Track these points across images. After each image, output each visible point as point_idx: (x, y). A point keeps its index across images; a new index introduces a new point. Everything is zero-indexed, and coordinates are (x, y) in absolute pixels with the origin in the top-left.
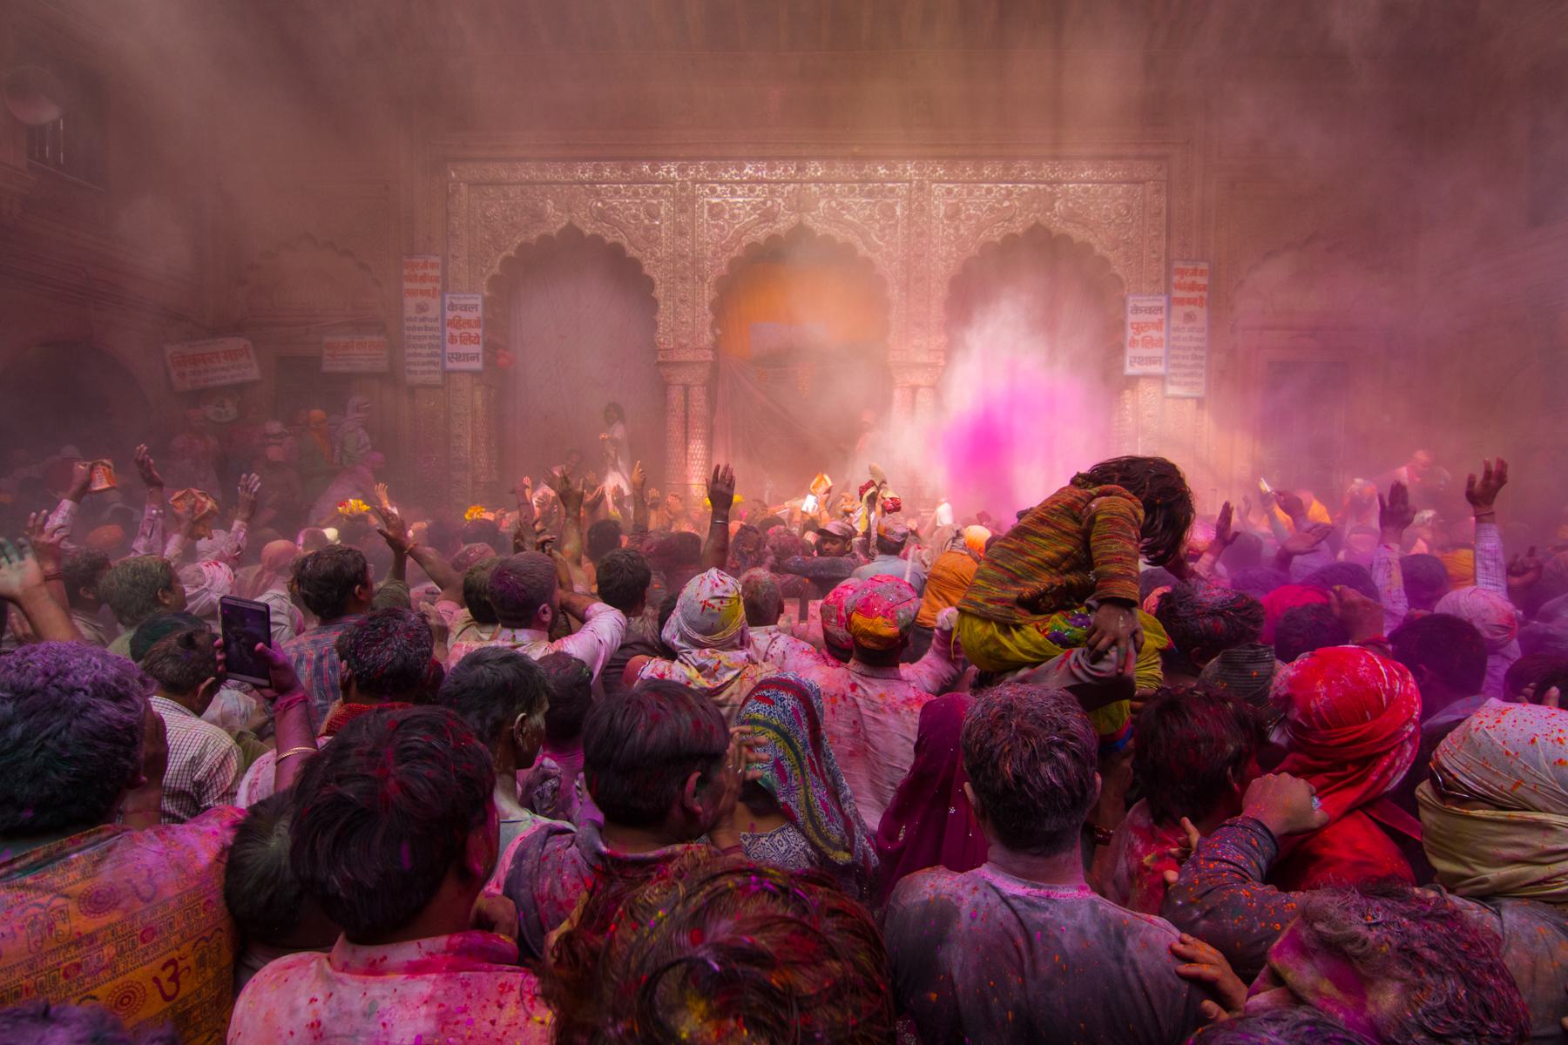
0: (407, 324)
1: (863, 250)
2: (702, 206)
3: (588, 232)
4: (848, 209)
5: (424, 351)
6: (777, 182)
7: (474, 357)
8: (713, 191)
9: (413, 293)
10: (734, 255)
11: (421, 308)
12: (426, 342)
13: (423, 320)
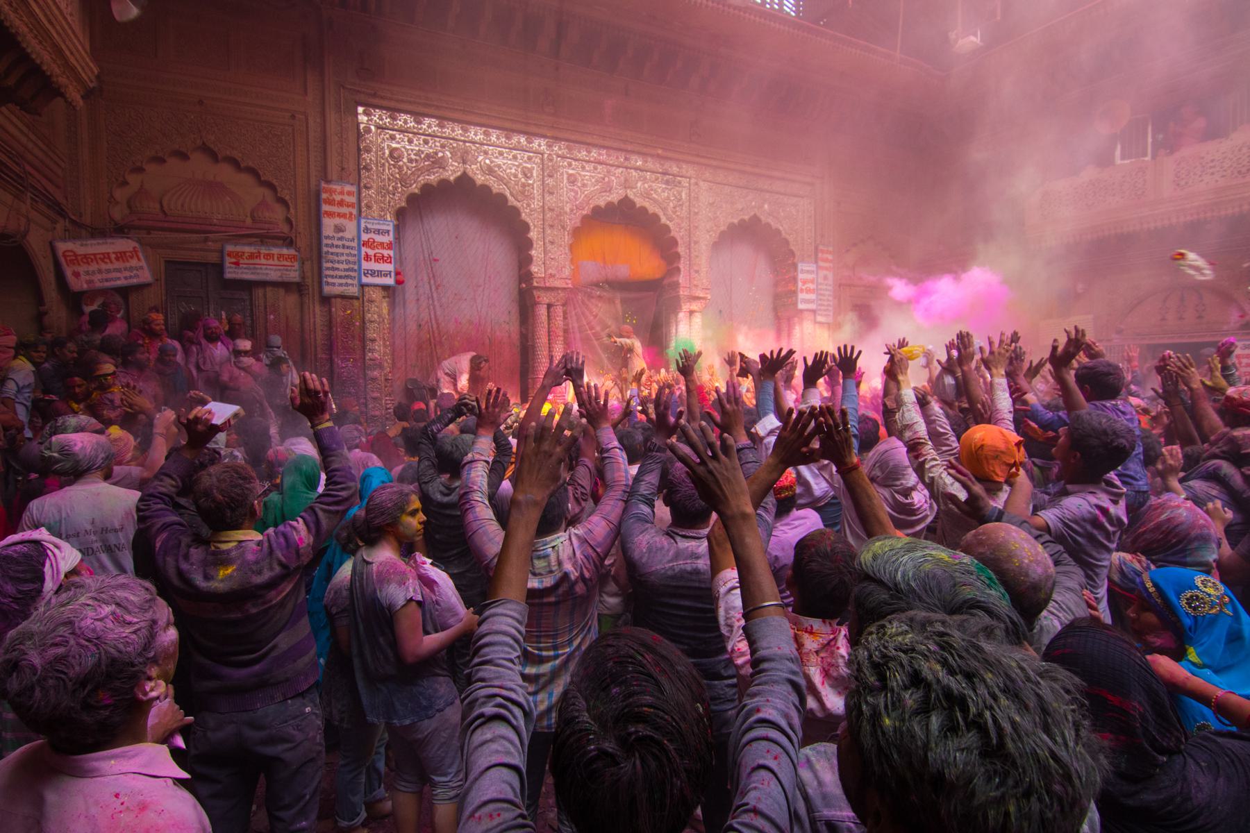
0: (325, 241)
1: (664, 220)
3: (479, 182)
4: (656, 191)
5: (341, 266)
8: (570, 165)
9: (330, 214)
10: (585, 212)
11: (339, 229)
13: (341, 239)
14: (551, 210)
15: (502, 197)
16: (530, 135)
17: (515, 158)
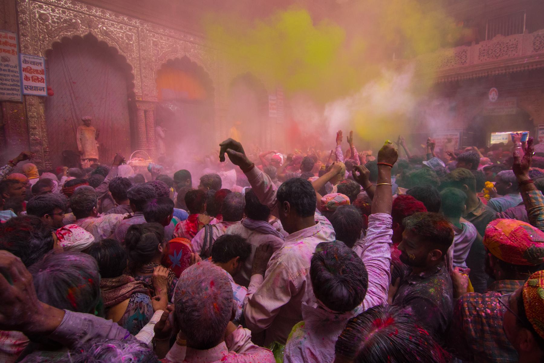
2: (149, 40)
6: (177, 39)
7: (42, 89)
12: (9, 78)
14: (145, 59)
15: (114, 50)
16: (131, 17)
17: (121, 28)
